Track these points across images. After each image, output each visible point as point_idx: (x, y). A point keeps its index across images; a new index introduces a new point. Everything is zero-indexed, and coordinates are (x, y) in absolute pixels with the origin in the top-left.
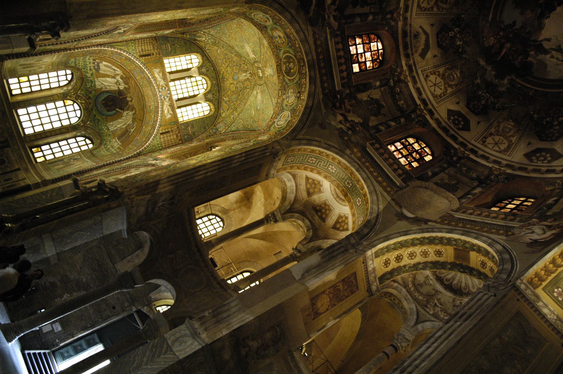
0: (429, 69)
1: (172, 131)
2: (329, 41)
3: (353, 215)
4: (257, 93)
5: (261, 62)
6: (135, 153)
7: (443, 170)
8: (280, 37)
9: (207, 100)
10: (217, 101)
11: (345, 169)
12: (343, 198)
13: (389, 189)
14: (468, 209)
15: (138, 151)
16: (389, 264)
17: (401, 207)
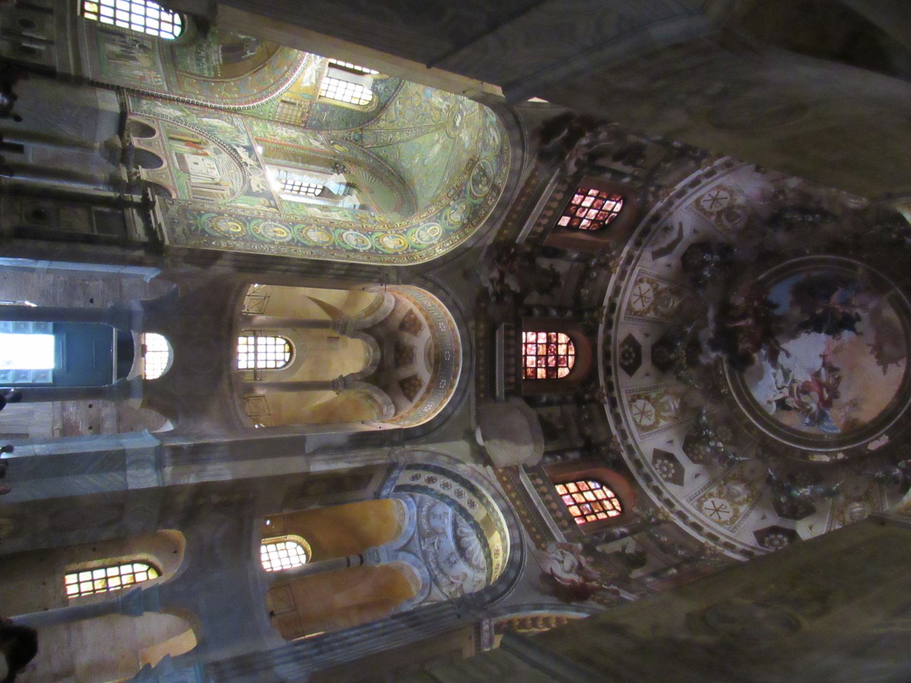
0: (649, 275)
1: (300, 105)
2: (549, 185)
3: (428, 390)
4: (438, 141)
5: (469, 112)
6: (232, 107)
7: (561, 403)
8: (494, 139)
9: (374, 89)
10: (386, 98)
11: (454, 340)
12: (433, 361)
13: (482, 395)
14: (541, 476)
15: (237, 107)
16: (418, 479)
17: (478, 423)
